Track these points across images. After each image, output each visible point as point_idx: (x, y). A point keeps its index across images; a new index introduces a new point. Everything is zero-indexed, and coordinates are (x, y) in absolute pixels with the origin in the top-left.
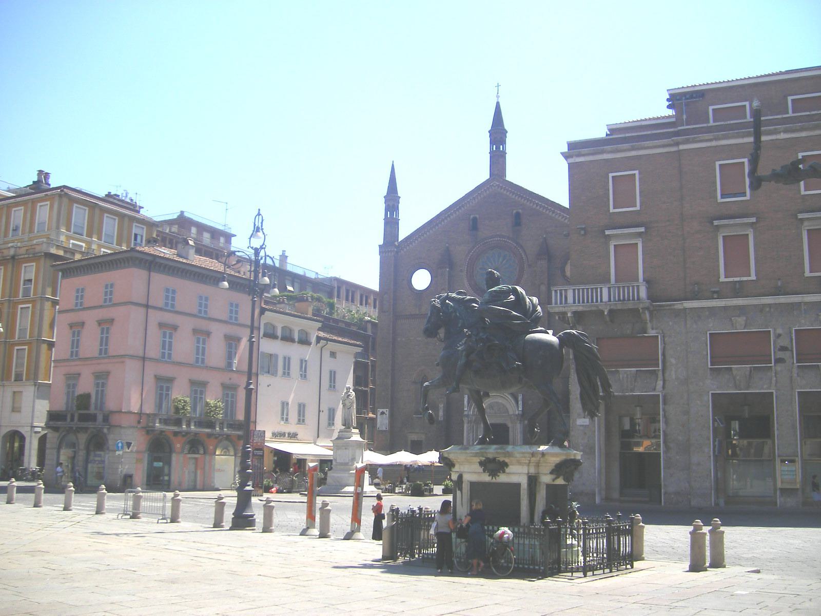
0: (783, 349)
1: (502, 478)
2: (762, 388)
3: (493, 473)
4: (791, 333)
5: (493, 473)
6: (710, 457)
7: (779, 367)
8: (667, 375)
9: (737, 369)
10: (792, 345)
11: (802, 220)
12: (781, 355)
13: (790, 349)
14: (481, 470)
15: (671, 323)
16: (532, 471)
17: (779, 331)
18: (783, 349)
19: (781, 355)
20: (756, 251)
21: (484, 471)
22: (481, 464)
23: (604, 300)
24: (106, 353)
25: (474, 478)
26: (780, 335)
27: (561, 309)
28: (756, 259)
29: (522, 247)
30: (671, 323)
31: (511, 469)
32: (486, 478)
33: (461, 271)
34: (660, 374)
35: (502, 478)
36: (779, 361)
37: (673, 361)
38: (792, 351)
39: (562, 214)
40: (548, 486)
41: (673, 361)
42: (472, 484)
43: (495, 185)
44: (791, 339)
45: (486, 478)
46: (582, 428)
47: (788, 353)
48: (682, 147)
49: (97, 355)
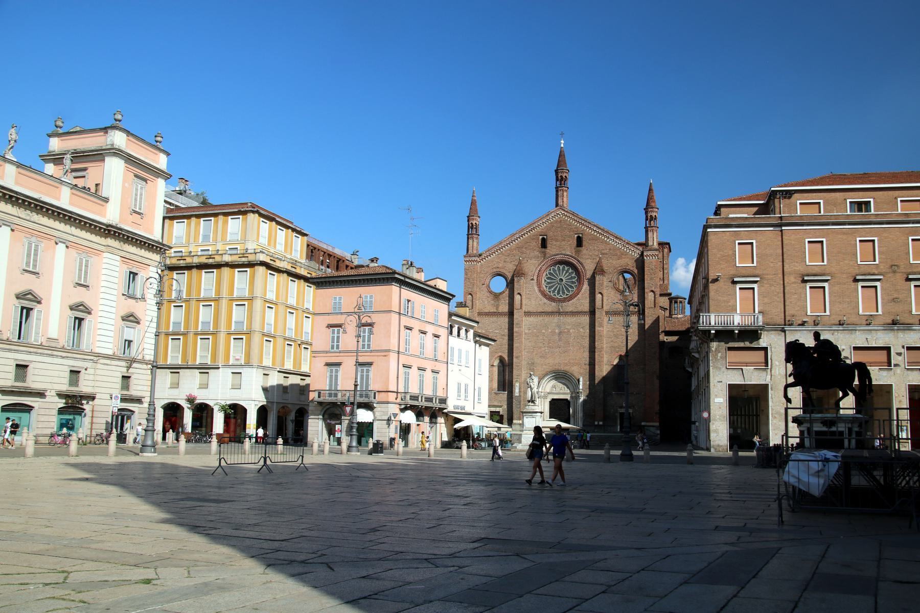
1: (834, 429)
8: (773, 372)
13: (850, 358)
14: (822, 425)
15: (776, 340)
16: (850, 425)
20: (830, 297)
21: (823, 426)
22: (822, 423)
24: (369, 347)
27: (707, 328)
28: (830, 302)
29: (581, 264)
30: (776, 340)
31: (840, 425)
33: (532, 280)
34: (769, 370)
35: (834, 429)
37: (777, 363)
39: (615, 240)
40: (857, 432)
41: (777, 363)
43: (560, 213)
45: (825, 429)
46: (718, 404)
48: (783, 228)
49: (329, 348)
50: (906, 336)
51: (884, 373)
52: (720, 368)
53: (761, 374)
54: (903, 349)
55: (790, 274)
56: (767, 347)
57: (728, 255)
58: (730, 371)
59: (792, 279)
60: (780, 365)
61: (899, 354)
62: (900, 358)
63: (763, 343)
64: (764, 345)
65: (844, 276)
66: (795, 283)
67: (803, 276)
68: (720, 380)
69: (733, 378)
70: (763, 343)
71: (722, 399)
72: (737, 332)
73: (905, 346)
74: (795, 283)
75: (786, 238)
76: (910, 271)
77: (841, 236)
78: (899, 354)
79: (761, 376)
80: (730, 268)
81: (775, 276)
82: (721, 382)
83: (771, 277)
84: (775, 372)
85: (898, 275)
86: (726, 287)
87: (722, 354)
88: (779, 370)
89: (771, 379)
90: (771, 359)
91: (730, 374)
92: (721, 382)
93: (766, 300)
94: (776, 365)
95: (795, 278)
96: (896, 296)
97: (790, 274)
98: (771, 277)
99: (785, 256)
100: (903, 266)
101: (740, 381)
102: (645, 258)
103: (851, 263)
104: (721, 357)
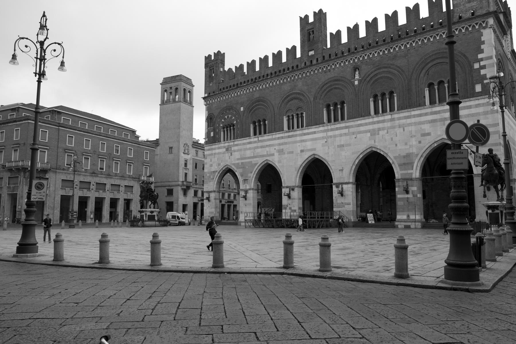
0: (76, 185)
1: (153, 214)
3: (152, 213)
5: (152, 213)
11: (83, 155)
12: (76, 186)
17: (76, 181)
18: (76, 185)
19: (76, 186)
25: (149, 214)
32: (151, 214)
35: (153, 214)
37: (52, 185)
41: (52, 185)
42: (148, 215)
47: (77, 186)
48: (60, 128)
50: (96, 178)
51: (88, 192)
59: (61, 150)
61: (93, 185)
62: (93, 187)
64: (47, 177)
65: (79, 152)
66: (62, 152)
67: (65, 150)
74: (62, 152)
76: (99, 154)
78: (93, 185)
85: (96, 155)
96: (94, 163)
100: (97, 152)
103: (82, 148)
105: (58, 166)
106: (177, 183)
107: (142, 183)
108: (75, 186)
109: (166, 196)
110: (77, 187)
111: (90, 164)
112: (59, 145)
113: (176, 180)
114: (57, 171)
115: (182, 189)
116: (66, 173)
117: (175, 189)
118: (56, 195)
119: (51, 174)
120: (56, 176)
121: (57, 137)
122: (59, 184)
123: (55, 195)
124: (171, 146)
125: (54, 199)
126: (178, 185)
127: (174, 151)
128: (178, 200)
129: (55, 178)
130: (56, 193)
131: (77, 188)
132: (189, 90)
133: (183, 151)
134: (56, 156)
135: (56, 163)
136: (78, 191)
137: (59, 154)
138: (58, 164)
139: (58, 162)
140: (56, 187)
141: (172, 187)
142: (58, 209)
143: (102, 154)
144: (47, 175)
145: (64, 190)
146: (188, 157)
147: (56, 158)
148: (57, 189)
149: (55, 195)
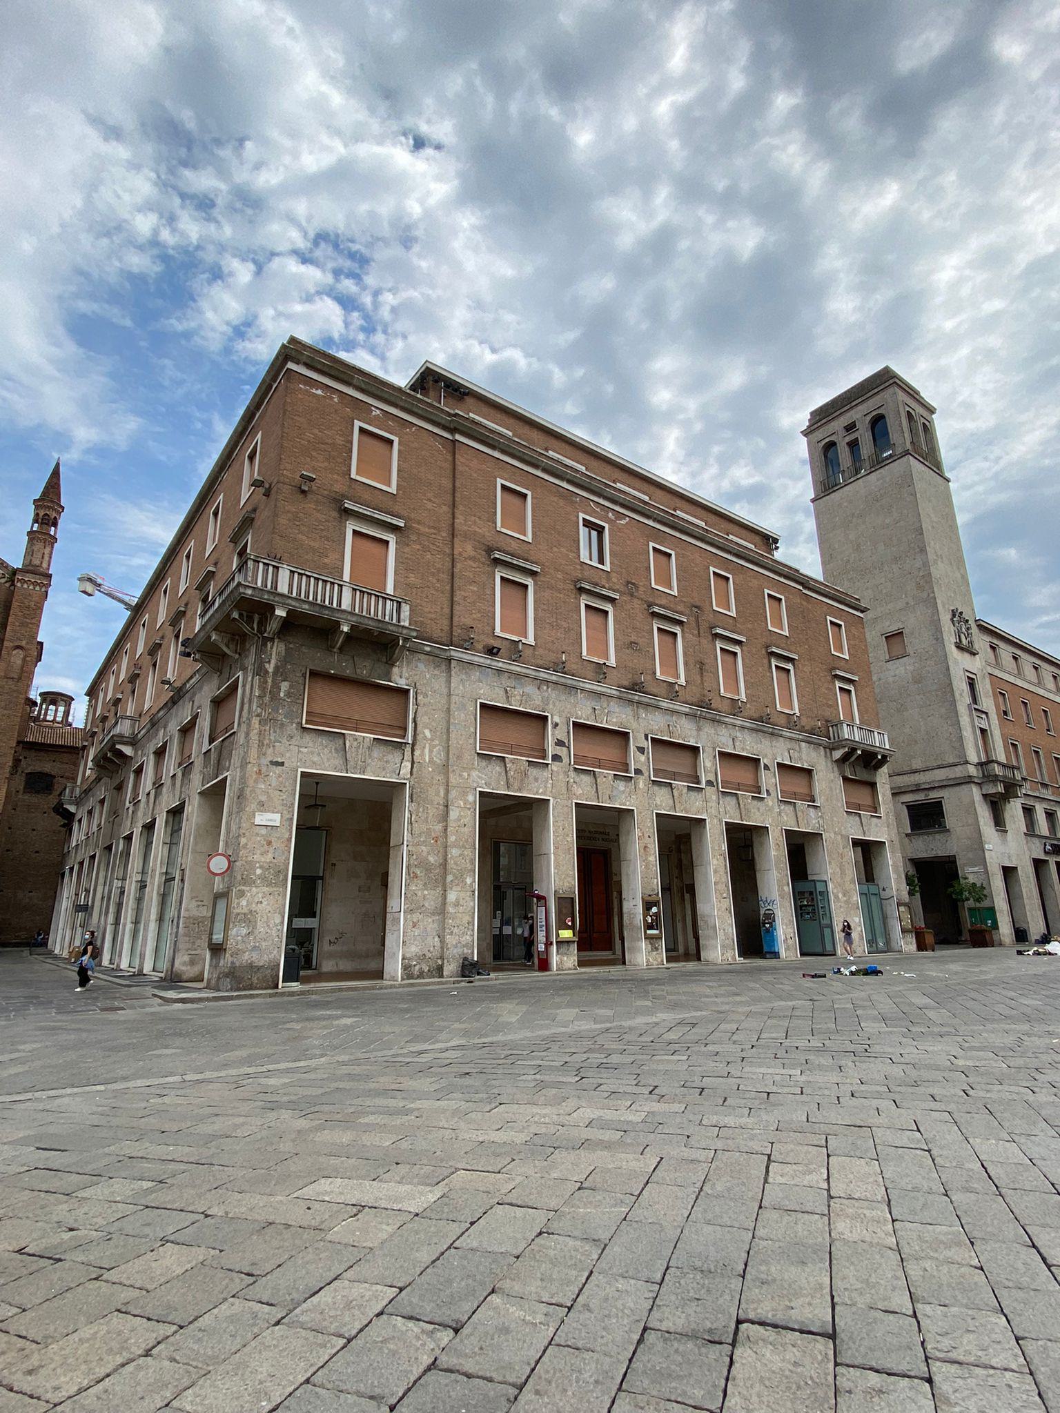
2: (537, 793)
4: (569, 726)
6: (474, 891)
7: (555, 767)
8: (417, 753)
9: (512, 761)
10: (569, 741)
13: (566, 741)
17: (556, 719)
18: (560, 743)
23: (344, 607)
26: (557, 725)
36: (556, 758)
37: (427, 733)
38: (569, 748)
41: (427, 733)
44: (568, 732)
46: (264, 831)
47: (565, 749)
50: (650, 716)
51: (621, 785)
52: (282, 725)
53: (390, 757)
54: (646, 742)
55: (466, 536)
56: (408, 691)
57: (334, 443)
58: (308, 738)
60: (432, 740)
61: (641, 750)
62: (643, 758)
63: (400, 677)
64: (402, 683)
68: (280, 760)
69: (316, 759)
70: (400, 677)
71: (277, 817)
72: (345, 629)
73: (650, 736)
75: (463, 460)
77: (555, 499)
78: (641, 750)
79: (387, 762)
80: (335, 476)
81: (433, 531)
82: (282, 764)
83: (427, 530)
84: (422, 755)
86: (322, 517)
87: (291, 687)
88: (431, 751)
89: (411, 773)
90: (415, 721)
91: (311, 744)
92: (282, 764)
93: (412, 579)
94: (425, 738)
95: (475, 548)
96: (633, 638)
97: (466, 536)
98: (427, 530)
99: (458, 495)
100: (642, 589)
101: (335, 769)
102: (19, 585)
103: (572, 555)
104: (288, 694)
105: (457, 631)
106: (958, 772)
107: (844, 759)
108: (551, 750)
109: (907, 835)
110: (562, 752)
111: (616, 639)
112: (460, 520)
113: (951, 759)
114: (455, 653)
115: (985, 796)
116: (500, 671)
117: (951, 801)
118: (453, 794)
119: (421, 666)
120: (449, 682)
121: (447, 483)
122: (468, 726)
123: (447, 791)
124: (893, 628)
125: (445, 817)
126: (969, 780)
127: (917, 642)
128: (983, 850)
129: (445, 691)
130: (453, 779)
131: (566, 760)
132: (923, 420)
133: (953, 640)
134: (445, 577)
135: (447, 611)
136: (572, 774)
137: (459, 566)
138: (455, 619)
139: (456, 607)
140: (453, 742)
141: (933, 795)
142: (469, 881)
143: (663, 602)
144: (395, 670)
145: (497, 768)
146: (975, 665)
147: (448, 588)
148: (459, 757)
149: (447, 791)
